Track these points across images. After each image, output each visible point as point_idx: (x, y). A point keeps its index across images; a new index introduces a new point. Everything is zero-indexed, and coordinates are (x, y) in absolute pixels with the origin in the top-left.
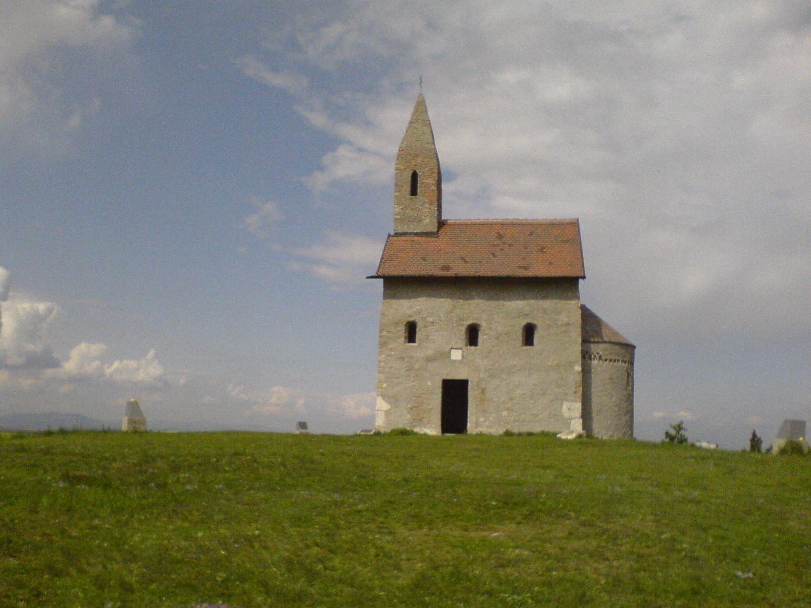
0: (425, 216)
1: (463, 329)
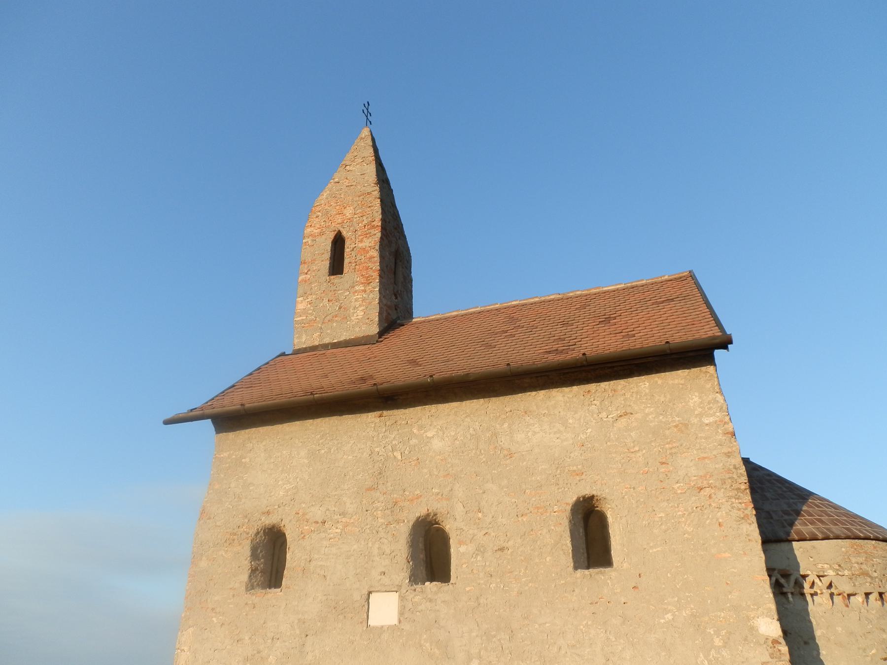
0: (355, 308)
1: (404, 530)
